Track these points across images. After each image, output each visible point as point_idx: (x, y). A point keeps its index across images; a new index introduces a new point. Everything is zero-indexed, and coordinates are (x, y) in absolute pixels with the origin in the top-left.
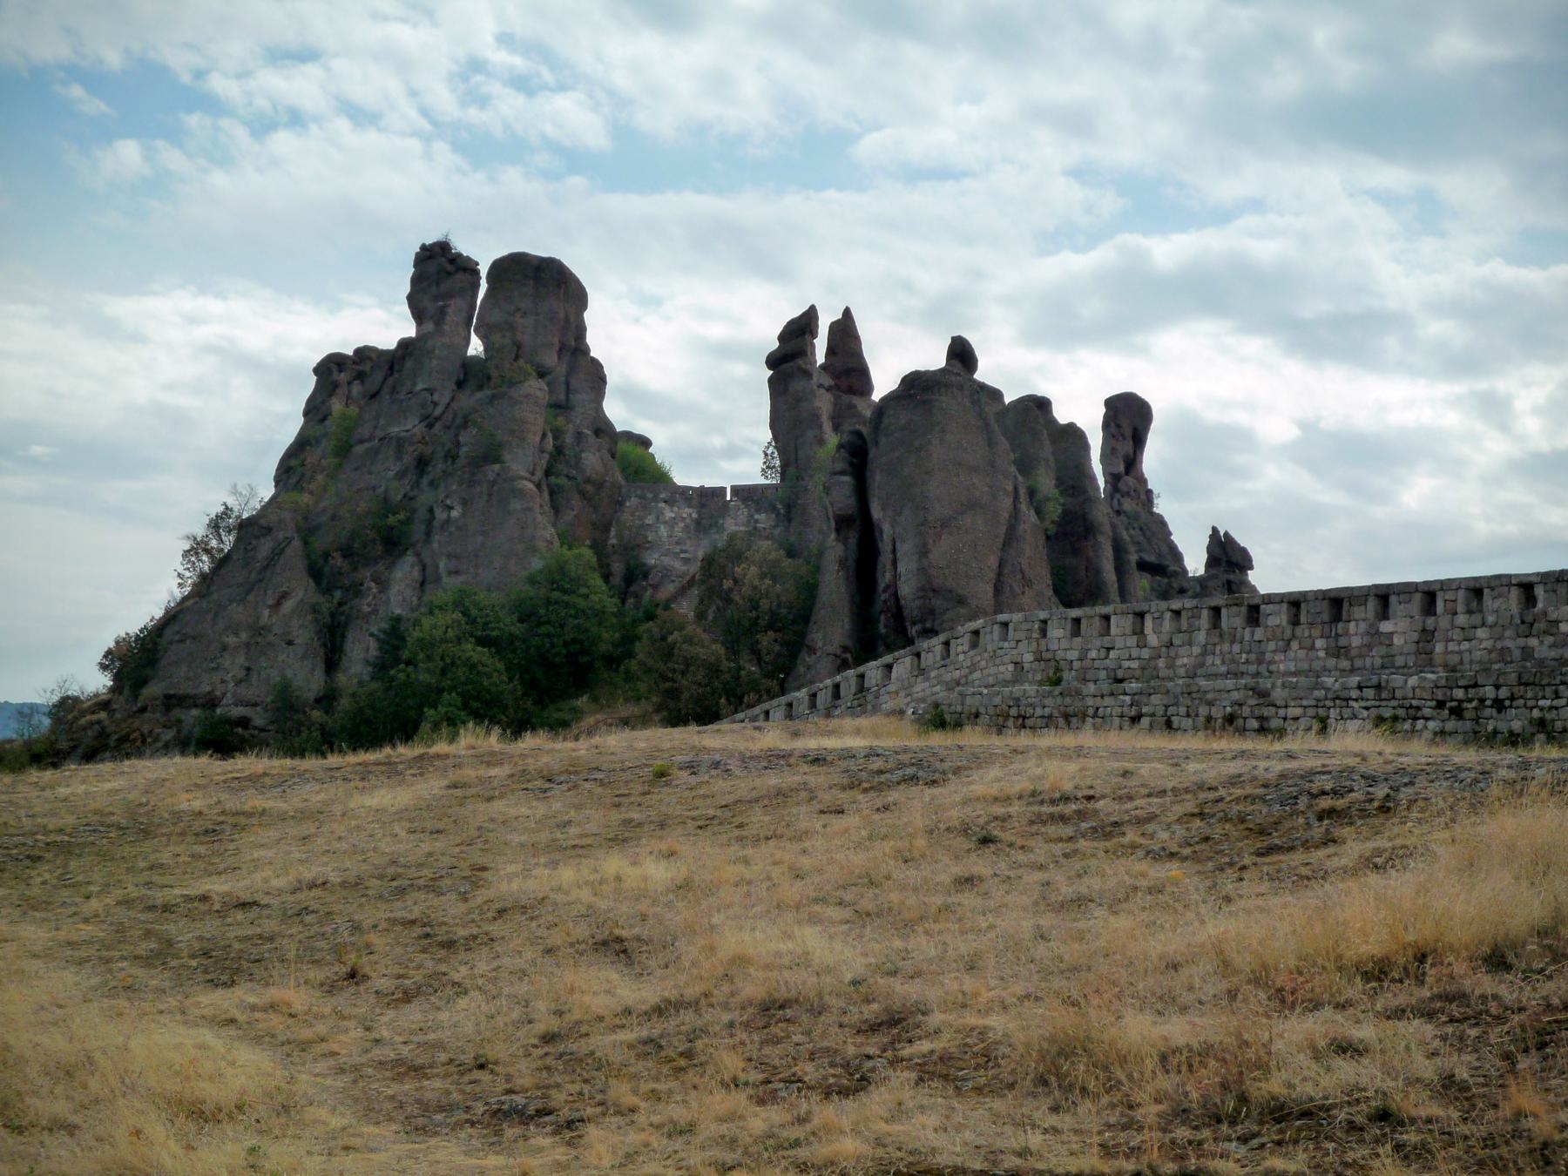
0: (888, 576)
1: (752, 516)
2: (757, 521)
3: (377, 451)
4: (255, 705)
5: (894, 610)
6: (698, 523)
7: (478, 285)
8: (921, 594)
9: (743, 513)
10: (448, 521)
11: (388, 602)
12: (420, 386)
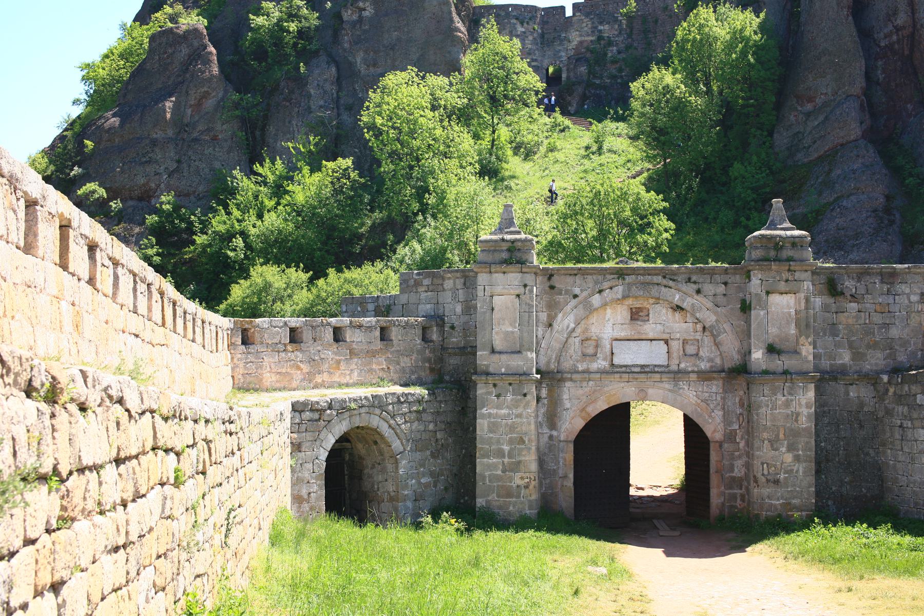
0: (902, 19)
1: (594, 28)
2: (600, 31)
4: (187, 195)
5: (907, 52)
6: (542, 36)
9: (587, 24)
10: (361, 20)
11: (309, 96)
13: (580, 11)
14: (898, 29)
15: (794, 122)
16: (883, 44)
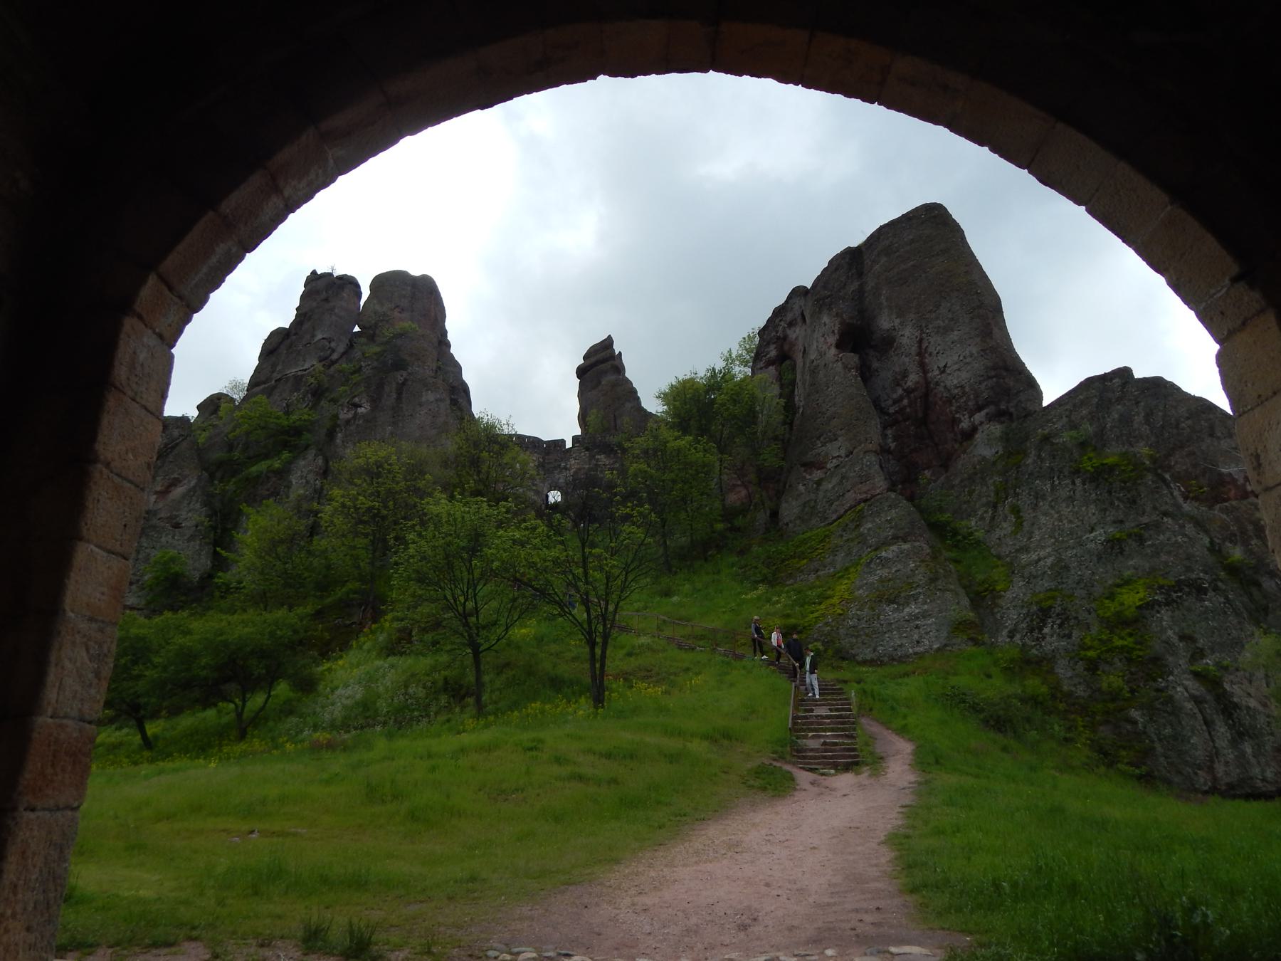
3: (274, 388)
5: (920, 415)
7: (359, 295)
8: (993, 373)
10: (356, 414)
12: (319, 336)
13: (579, 442)
14: (909, 392)
15: (803, 491)
16: (891, 410)
